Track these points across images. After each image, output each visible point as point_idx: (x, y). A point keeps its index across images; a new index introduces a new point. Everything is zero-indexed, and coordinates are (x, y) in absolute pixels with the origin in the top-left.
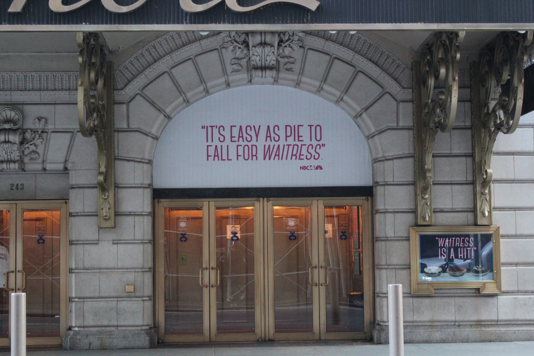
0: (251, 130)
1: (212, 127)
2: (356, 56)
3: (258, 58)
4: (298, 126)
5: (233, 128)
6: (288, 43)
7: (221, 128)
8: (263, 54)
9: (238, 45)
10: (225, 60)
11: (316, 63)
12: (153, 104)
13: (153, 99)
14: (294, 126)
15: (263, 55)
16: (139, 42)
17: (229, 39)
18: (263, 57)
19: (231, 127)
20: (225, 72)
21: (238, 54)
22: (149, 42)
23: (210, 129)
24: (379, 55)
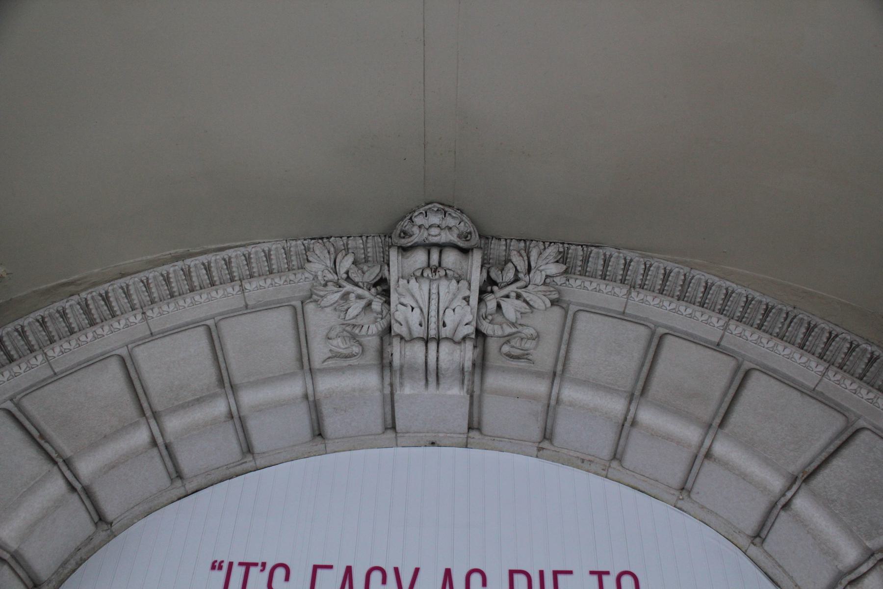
0: (384, 582)
1: (248, 566)
2: (732, 327)
3: (415, 318)
4: (556, 573)
5: (319, 571)
6: (513, 287)
7: (280, 573)
8: (434, 302)
9: (356, 288)
10: (311, 329)
11: (605, 346)
12: (38, 441)
13: (44, 426)
14: (541, 573)
15: (433, 307)
16: (64, 285)
17: (330, 276)
18: (433, 313)
19: (316, 568)
20: (304, 364)
21: (352, 312)
22: (94, 284)
23: (238, 573)
24: (803, 330)
